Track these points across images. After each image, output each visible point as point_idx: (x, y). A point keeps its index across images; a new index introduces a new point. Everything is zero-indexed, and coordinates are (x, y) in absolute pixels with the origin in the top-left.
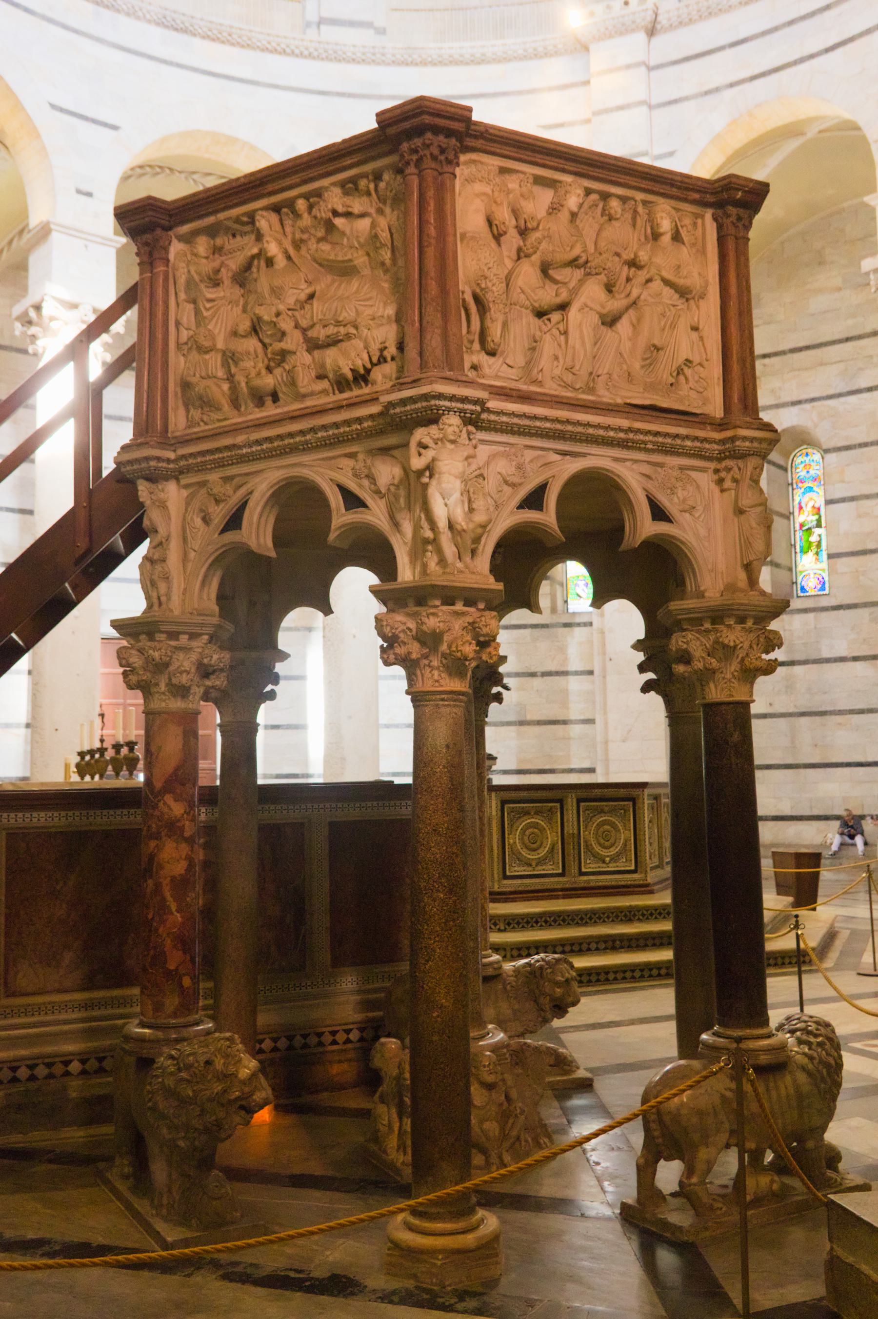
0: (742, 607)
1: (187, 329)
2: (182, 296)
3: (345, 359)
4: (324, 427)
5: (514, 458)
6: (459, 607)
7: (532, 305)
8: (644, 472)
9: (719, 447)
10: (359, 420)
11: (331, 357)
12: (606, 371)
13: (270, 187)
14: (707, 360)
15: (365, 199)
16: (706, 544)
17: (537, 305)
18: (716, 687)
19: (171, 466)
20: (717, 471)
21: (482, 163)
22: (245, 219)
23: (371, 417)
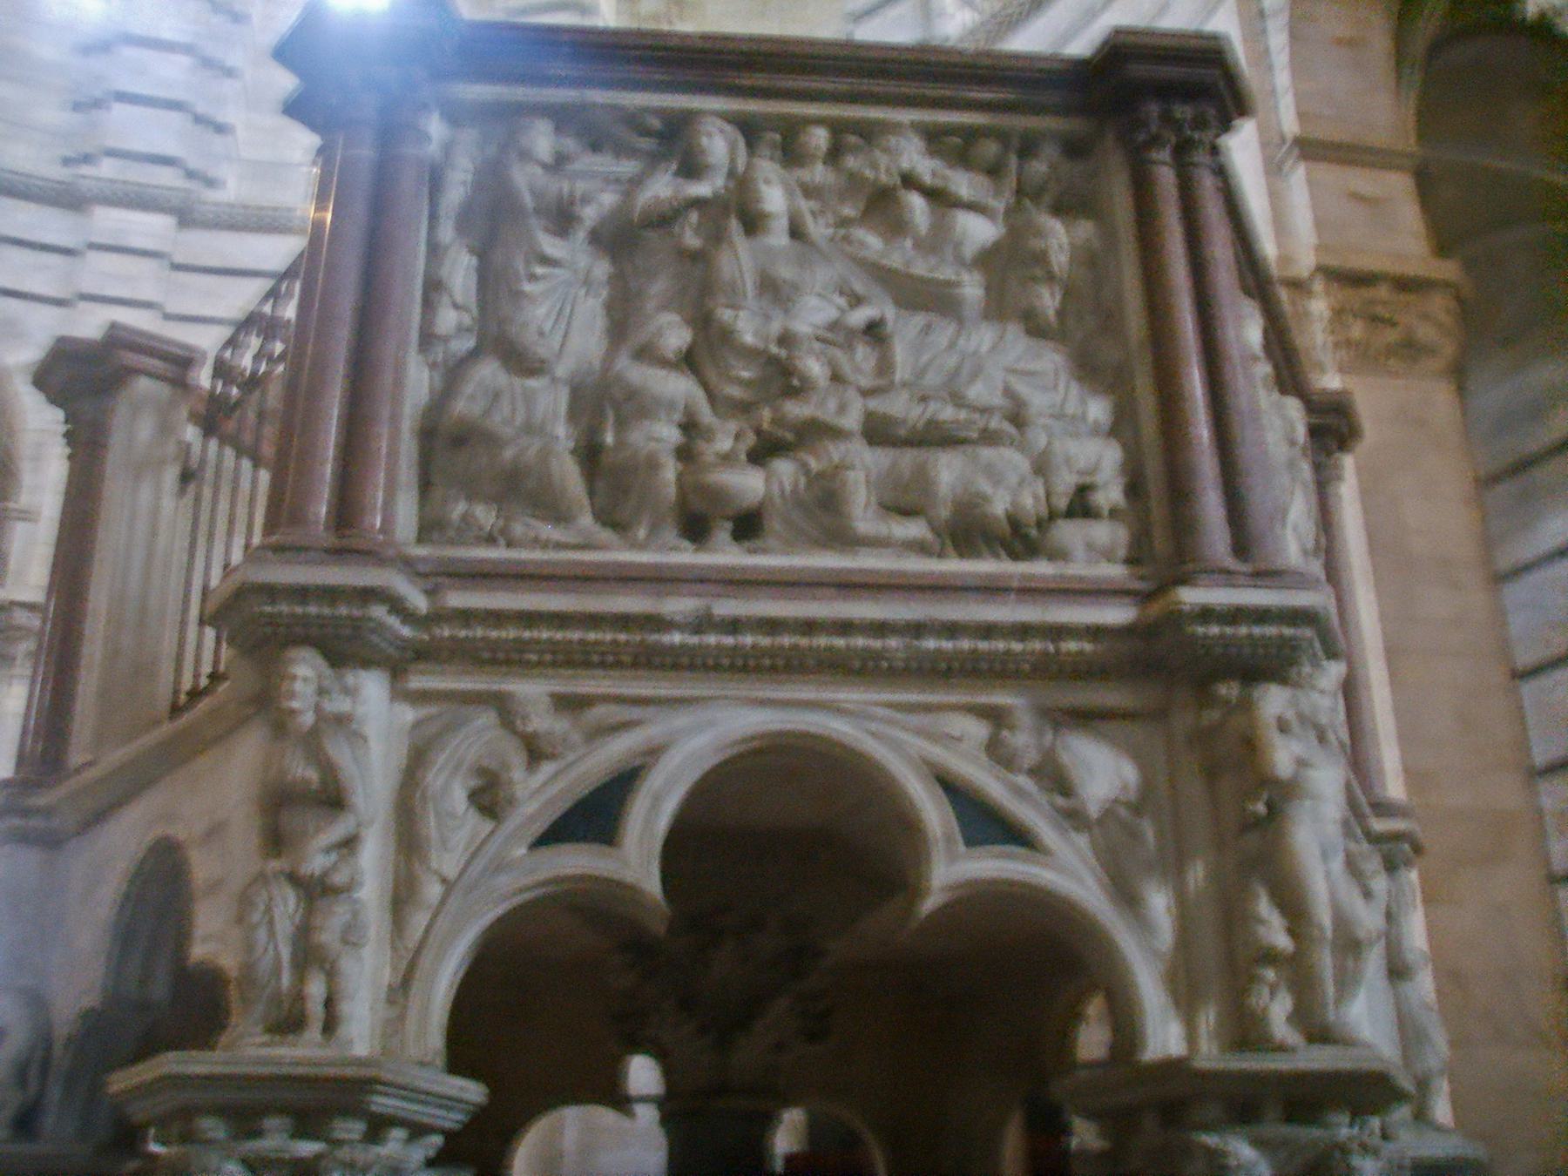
1: (456, 306)
2: (447, 233)
3: (1007, 488)
4: (952, 630)
10: (1058, 632)
11: (948, 472)
13: (760, 80)
15: (981, 180)
19: (406, 631)
22: (656, 123)
23: (1095, 632)
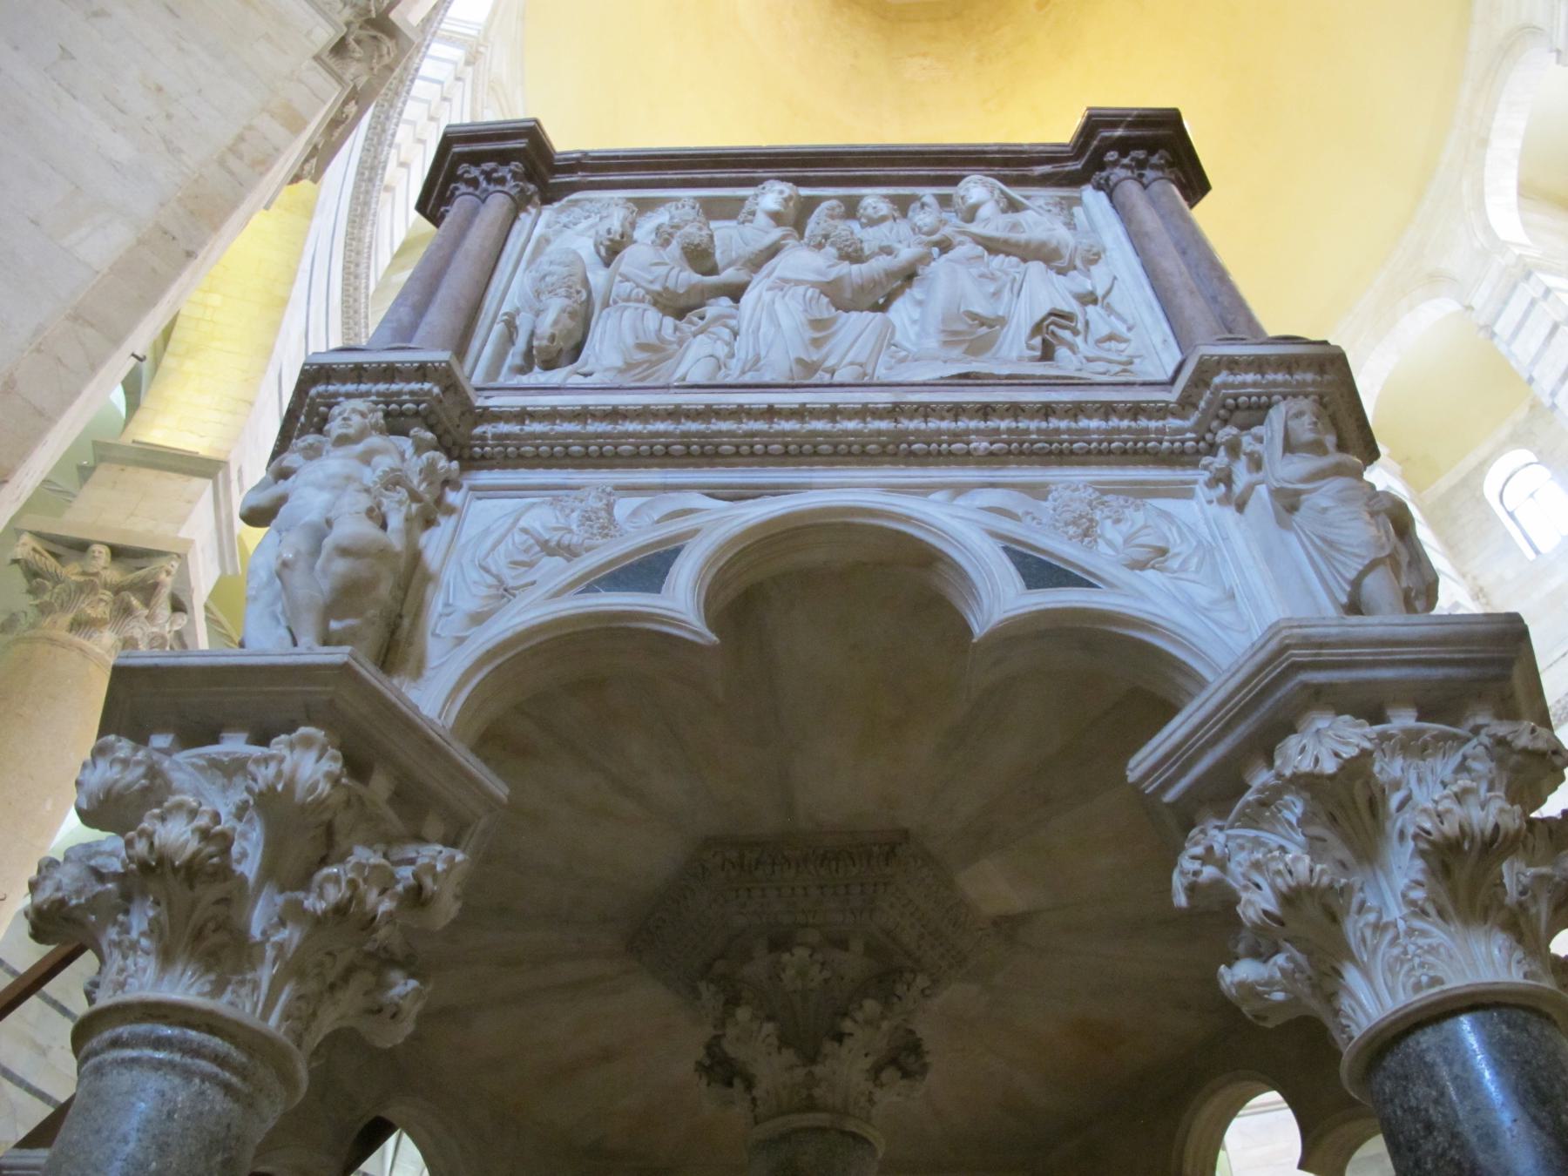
0: (1327, 654)
5: (577, 503)
6: (235, 745)
7: (648, 292)
8: (986, 505)
9: (1195, 416)
12: (848, 359)
14: (1130, 329)
16: (1227, 617)
17: (657, 287)
18: (1366, 973)
20: (1212, 483)
21: (591, 201)
